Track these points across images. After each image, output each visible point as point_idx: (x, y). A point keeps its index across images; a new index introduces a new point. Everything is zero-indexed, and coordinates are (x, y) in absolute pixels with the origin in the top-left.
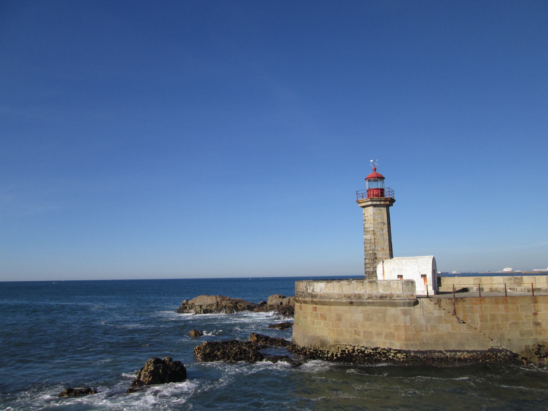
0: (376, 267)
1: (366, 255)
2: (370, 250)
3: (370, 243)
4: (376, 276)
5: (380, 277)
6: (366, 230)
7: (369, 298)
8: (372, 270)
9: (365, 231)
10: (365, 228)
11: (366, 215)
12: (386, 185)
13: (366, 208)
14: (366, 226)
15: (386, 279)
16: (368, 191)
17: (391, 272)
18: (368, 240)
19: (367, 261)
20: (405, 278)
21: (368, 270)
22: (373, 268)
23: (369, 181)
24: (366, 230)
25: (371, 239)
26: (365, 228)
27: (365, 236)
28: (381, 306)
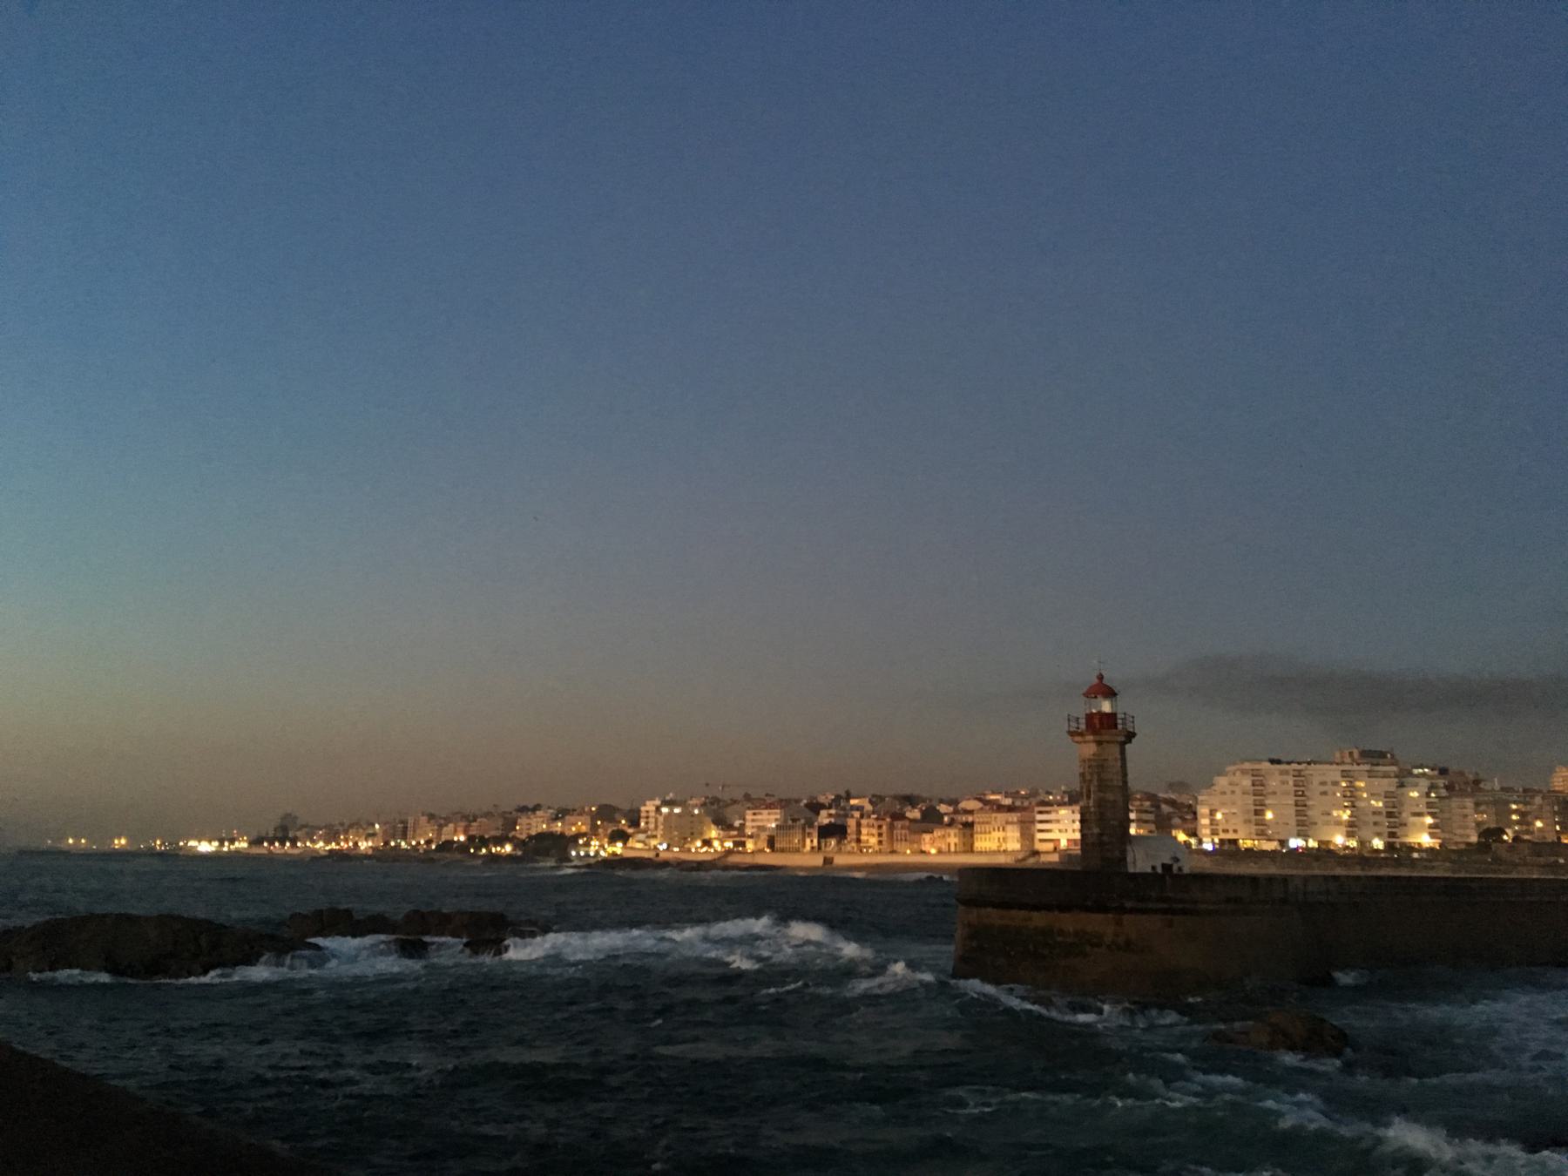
8: (1117, 853)
10: (1100, 780)
19: (1105, 838)
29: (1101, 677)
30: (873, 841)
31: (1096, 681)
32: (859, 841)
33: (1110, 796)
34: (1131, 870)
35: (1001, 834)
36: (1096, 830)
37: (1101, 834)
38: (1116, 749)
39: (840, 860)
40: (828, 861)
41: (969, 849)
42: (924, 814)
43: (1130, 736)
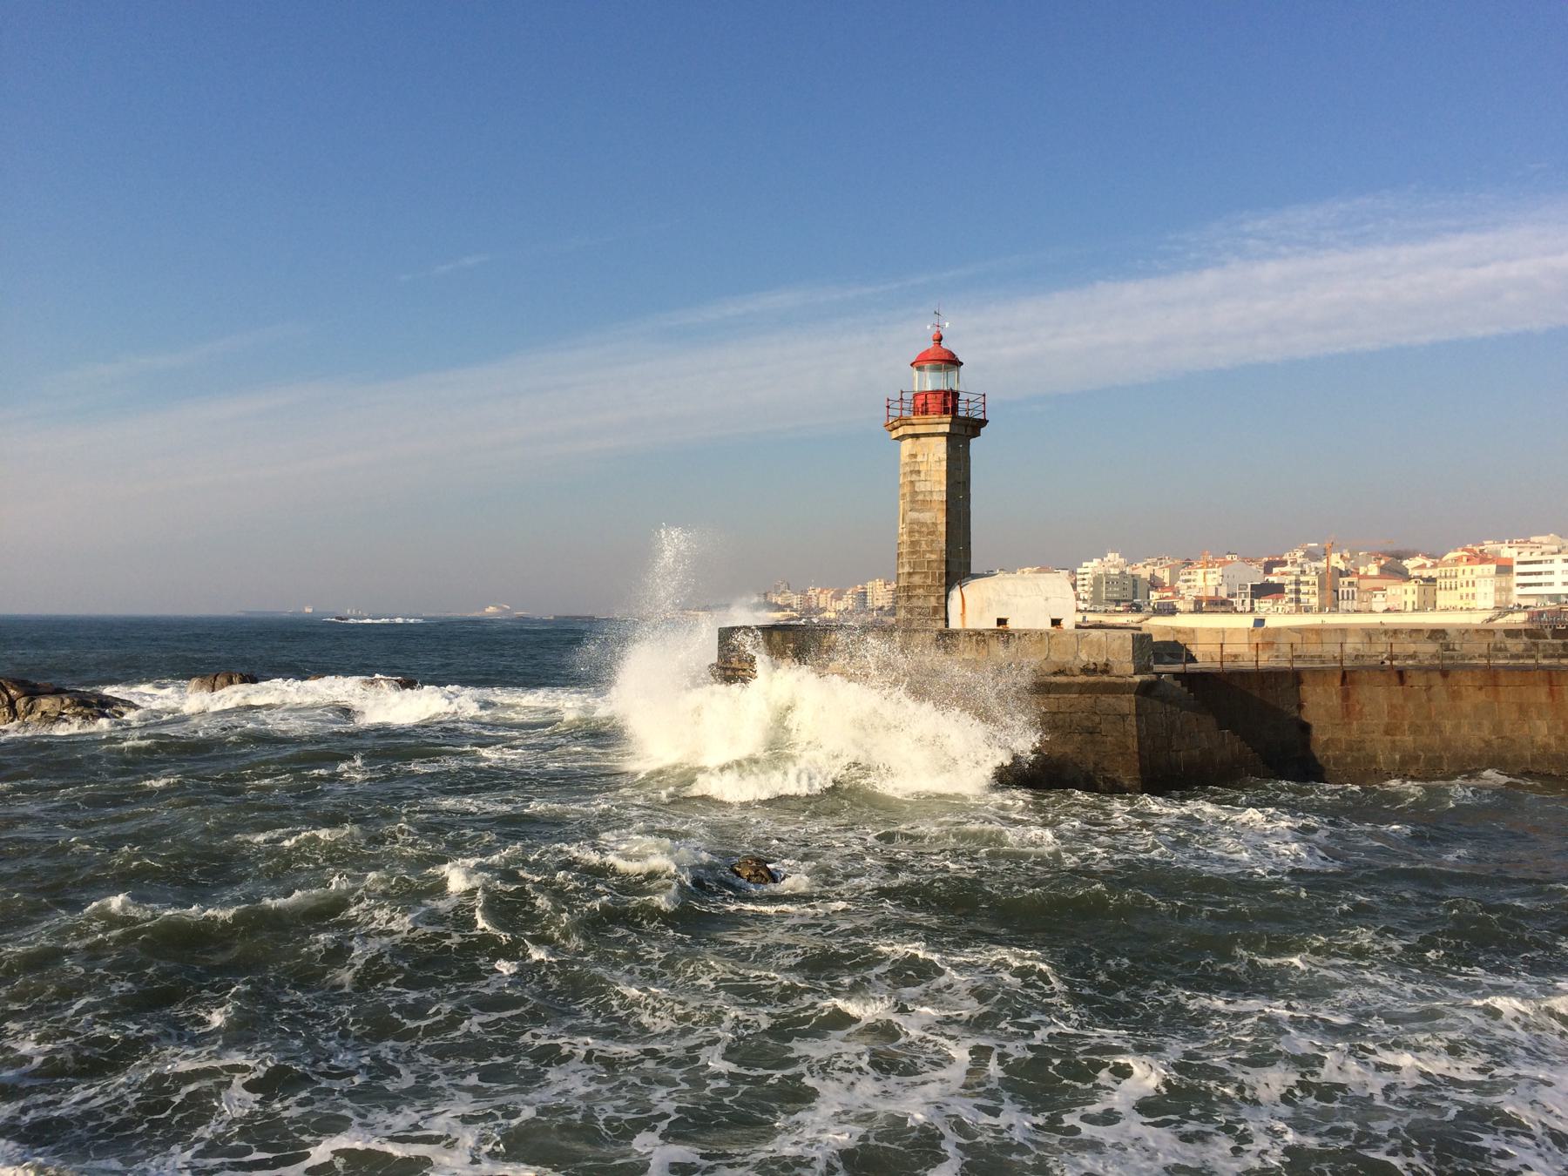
0: (947, 596)
1: (914, 565)
2: (931, 552)
3: (929, 533)
4: (947, 620)
5: (955, 624)
6: (920, 497)
7: (1055, 674)
8: (933, 602)
9: (913, 501)
10: (914, 493)
11: (919, 458)
12: (966, 383)
13: (923, 439)
14: (920, 487)
15: (969, 626)
16: (916, 395)
17: (981, 612)
18: (923, 524)
19: (917, 580)
20: (1011, 625)
21: (920, 603)
22: (939, 598)
23: (920, 369)
24: (920, 497)
25: (935, 524)
26: (914, 493)
27: (915, 515)
28: (1081, 693)
29: (940, 339)
30: (1314, 601)
31: (931, 344)
32: (1298, 601)
33: (927, 517)
34: (955, 624)
35: (1470, 590)
36: (907, 569)
37: (910, 574)
38: (939, 448)
39: (1272, 622)
40: (1259, 622)
41: (1427, 603)
42: (1382, 568)
43: (975, 426)
